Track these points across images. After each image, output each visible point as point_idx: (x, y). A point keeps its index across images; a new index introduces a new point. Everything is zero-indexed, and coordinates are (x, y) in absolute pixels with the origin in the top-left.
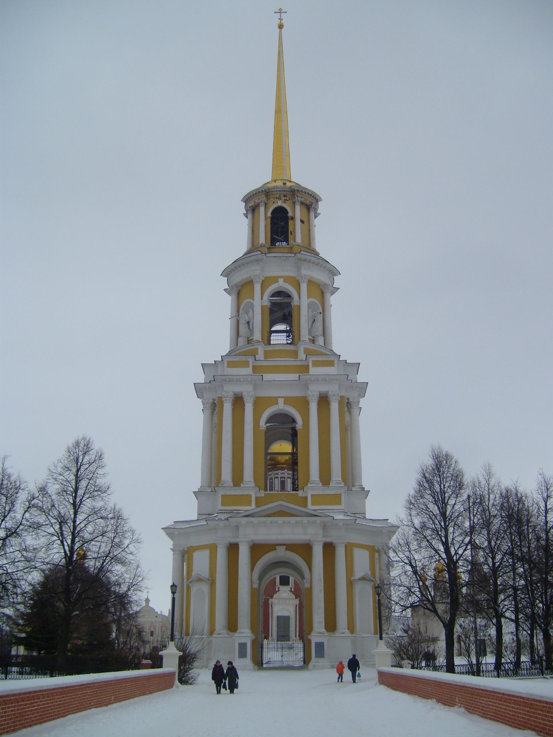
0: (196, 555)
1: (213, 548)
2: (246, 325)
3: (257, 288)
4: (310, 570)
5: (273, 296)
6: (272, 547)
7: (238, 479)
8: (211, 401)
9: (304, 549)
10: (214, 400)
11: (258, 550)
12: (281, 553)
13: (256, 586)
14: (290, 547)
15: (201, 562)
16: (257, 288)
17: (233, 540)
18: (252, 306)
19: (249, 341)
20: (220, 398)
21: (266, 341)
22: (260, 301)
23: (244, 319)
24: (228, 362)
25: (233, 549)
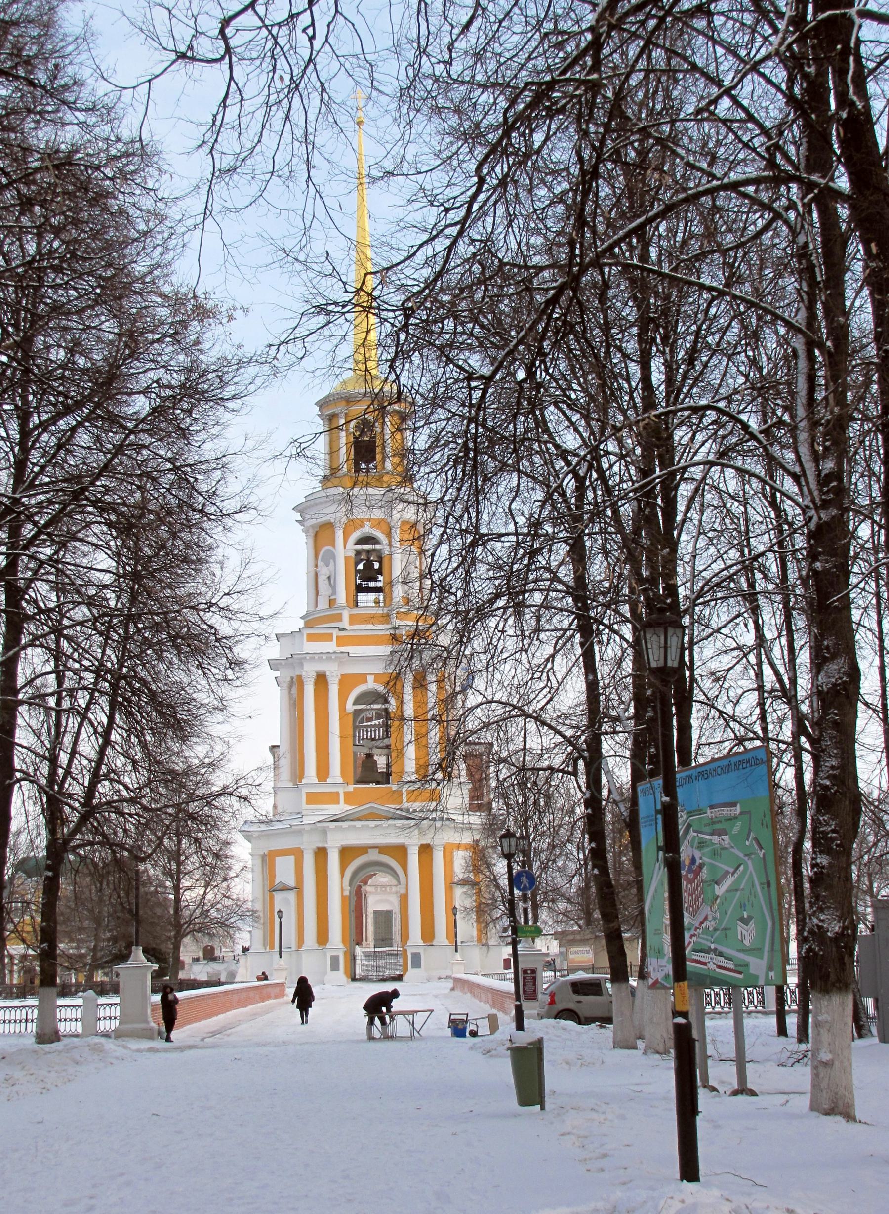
0: (279, 860)
1: (298, 854)
2: (327, 582)
3: (339, 534)
4: (406, 875)
5: (358, 542)
6: (363, 850)
7: (323, 772)
8: (289, 679)
9: (400, 852)
10: (292, 678)
11: (347, 853)
12: (373, 856)
13: (347, 893)
14: (383, 849)
15: (285, 870)
16: (339, 534)
17: (320, 845)
18: (333, 557)
19: (332, 602)
20: (300, 677)
21: (352, 603)
22: (344, 549)
23: (324, 572)
24: (308, 635)
25: (321, 854)
